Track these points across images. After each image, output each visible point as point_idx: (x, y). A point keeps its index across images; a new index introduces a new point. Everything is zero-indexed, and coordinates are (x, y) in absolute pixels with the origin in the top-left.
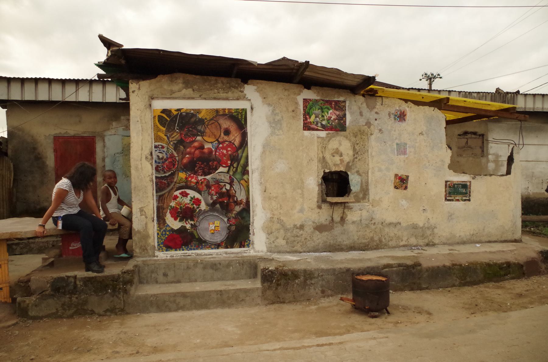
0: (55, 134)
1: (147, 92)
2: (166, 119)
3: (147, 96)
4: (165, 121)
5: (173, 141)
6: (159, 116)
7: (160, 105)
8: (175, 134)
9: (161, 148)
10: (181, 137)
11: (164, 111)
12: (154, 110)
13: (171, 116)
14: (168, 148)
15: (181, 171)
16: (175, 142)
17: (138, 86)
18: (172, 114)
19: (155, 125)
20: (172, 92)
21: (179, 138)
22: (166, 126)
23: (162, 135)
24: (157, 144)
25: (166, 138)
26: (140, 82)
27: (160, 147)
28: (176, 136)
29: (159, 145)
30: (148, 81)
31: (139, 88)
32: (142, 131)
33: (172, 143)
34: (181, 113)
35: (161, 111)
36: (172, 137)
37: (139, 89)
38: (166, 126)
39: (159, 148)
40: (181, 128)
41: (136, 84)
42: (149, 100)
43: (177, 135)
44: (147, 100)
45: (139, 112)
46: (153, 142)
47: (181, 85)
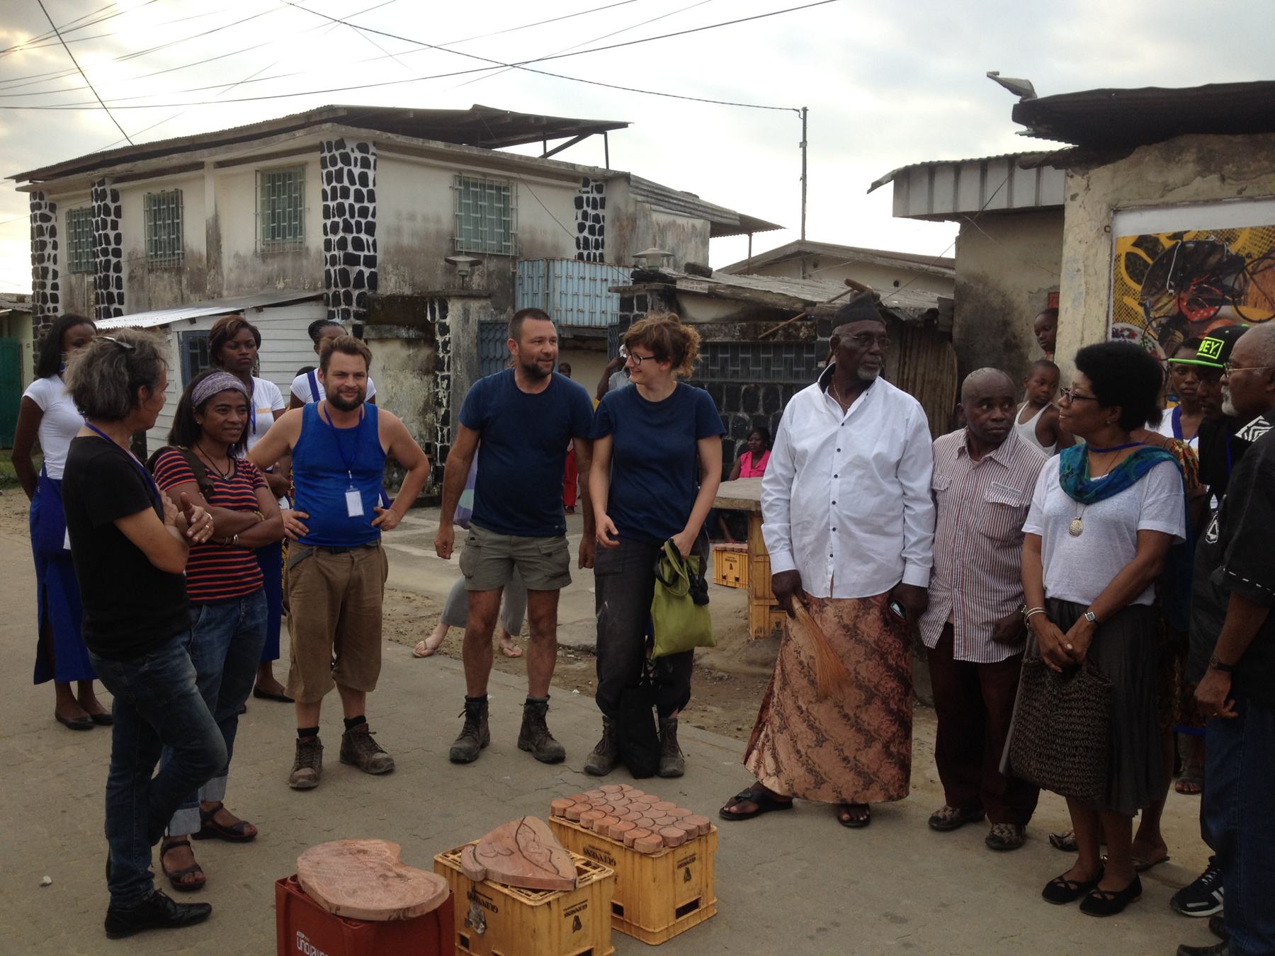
0: (1051, 288)
1: (1104, 195)
2: (1145, 262)
3: (1104, 207)
4: (1142, 268)
5: (1159, 320)
6: (1128, 254)
7: (1132, 225)
8: (1165, 300)
9: (1129, 337)
10: (1180, 308)
11: (1142, 241)
12: (1117, 239)
13: (1158, 254)
14: (1144, 338)
15: (1174, 398)
16: (1164, 321)
17: (1085, 182)
18: (1161, 248)
19: (1119, 279)
20: (1167, 188)
21: (1175, 311)
22: (1144, 280)
23: (1132, 303)
24: (1119, 326)
25: (1141, 310)
26: (1090, 172)
27: (1126, 333)
28: (1167, 305)
29: (1123, 330)
30: (1110, 166)
31: (1088, 186)
32: (1087, 293)
33: (1154, 324)
34: (1183, 244)
35: (1132, 242)
36: (1155, 308)
37: (1088, 188)
38: (1144, 280)
39: (1123, 336)
40: (1180, 285)
41: (1080, 178)
42: (1108, 214)
43: (1169, 302)
44: (1104, 214)
45: (1084, 246)
46: (1111, 321)
47: (1191, 167)
